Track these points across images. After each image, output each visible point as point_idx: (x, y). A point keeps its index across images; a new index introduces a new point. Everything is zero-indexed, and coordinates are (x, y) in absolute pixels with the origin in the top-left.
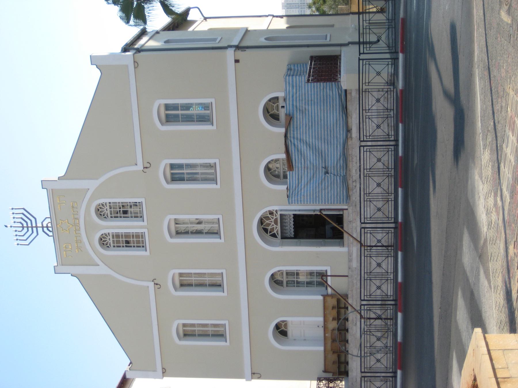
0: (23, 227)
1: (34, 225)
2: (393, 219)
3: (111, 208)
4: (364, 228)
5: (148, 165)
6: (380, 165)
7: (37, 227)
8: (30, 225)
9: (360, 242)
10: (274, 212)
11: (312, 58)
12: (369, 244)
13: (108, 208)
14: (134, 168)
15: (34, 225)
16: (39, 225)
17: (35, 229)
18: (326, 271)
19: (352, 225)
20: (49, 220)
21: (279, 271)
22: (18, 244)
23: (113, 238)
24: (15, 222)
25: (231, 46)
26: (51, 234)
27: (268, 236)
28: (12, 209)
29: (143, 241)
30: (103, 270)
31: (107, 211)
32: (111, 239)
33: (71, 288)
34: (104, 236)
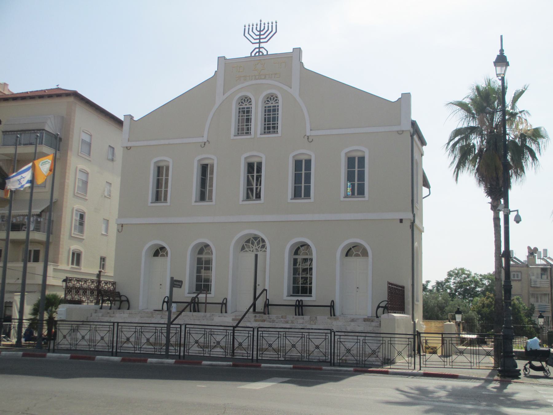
0: (260, 31)
1: (262, 41)
2: (261, 358)
3: (273, 106)
4: (253, 331)
5: (310, 140)
7: (260, 43)
8: (262, 37)
9: (237, 326)
10: (264, 249)
11: (403, 287)
12: (235, 334)
13: (274, 105)
15: (262, 41)
16: (262, 45)
17: (258, 41)
18: (210, 293)
20: (265, 53)
21: (212, 251)
22: (245, 26)
23: (247, 108)
24: (264, 24)
25: (414, 216)
26: (253, 54)
27: (243, 242)
28: (276, 23)
29: (243, 133)
31: (272, 104)
32: (246, 107)
34: (249, 100)
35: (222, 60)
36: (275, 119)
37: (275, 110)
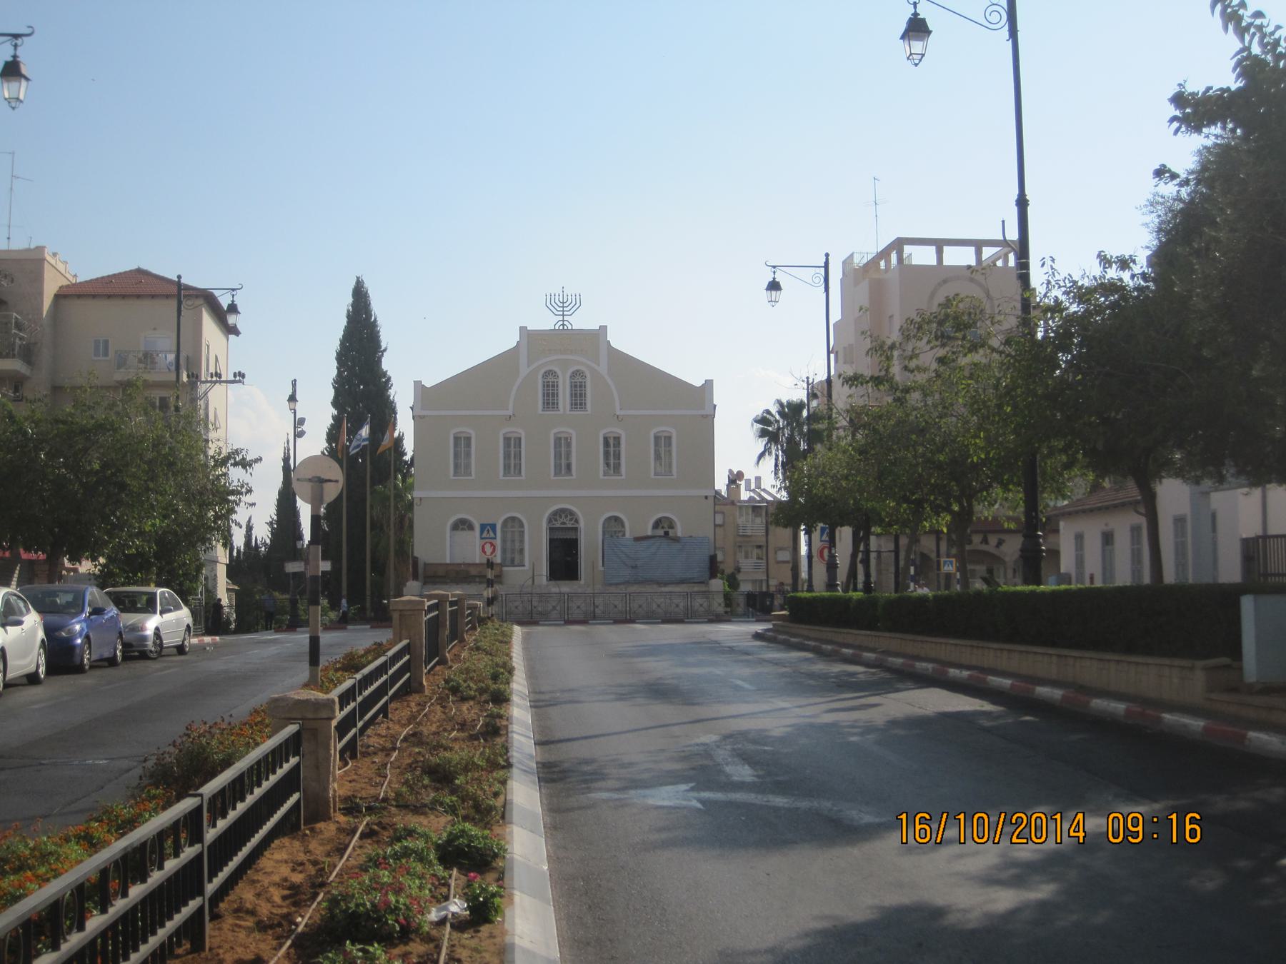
6: (655, 606)
14: (618, 407)
19: (566, 587)
30: (524, 370)
33: (509, 340)
35: (523, 329)
36: (583, 395)
37: (582, 386)
